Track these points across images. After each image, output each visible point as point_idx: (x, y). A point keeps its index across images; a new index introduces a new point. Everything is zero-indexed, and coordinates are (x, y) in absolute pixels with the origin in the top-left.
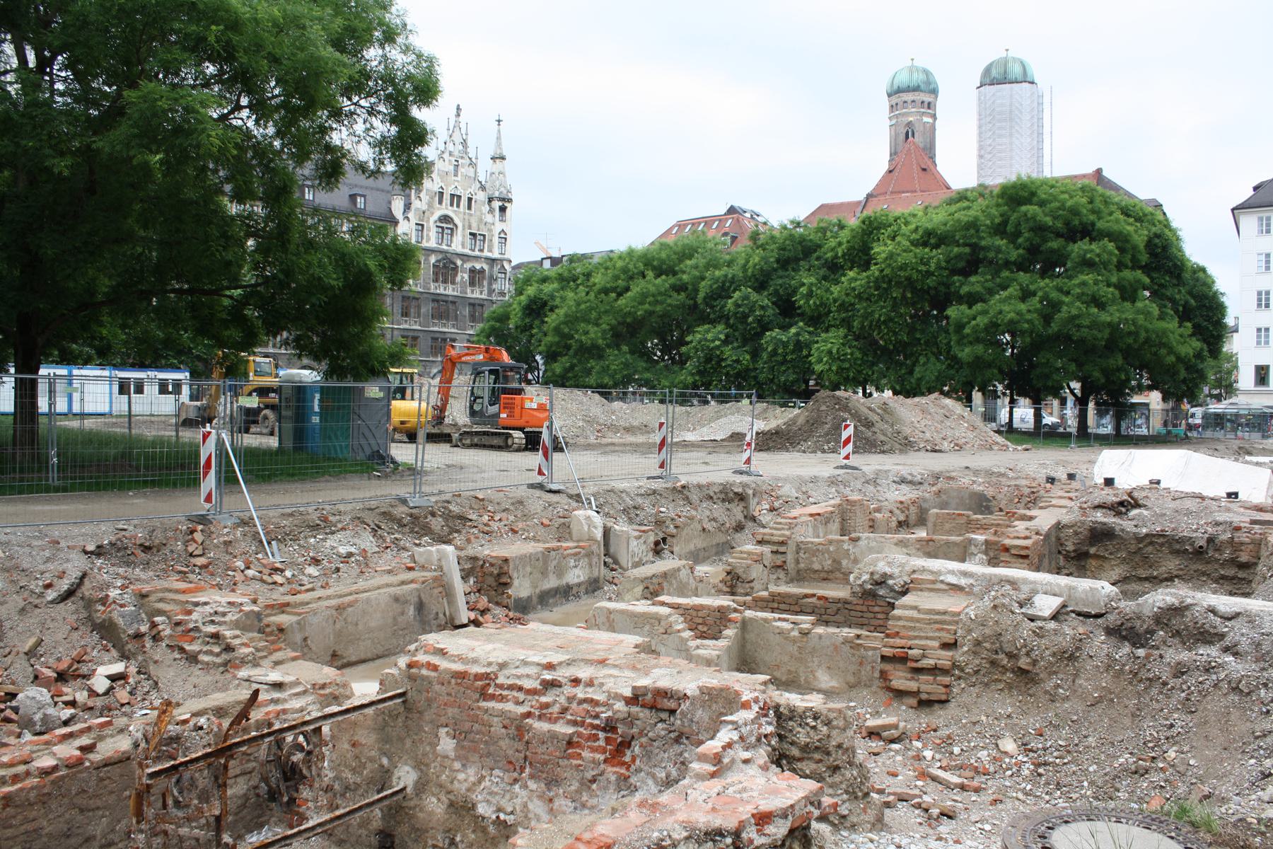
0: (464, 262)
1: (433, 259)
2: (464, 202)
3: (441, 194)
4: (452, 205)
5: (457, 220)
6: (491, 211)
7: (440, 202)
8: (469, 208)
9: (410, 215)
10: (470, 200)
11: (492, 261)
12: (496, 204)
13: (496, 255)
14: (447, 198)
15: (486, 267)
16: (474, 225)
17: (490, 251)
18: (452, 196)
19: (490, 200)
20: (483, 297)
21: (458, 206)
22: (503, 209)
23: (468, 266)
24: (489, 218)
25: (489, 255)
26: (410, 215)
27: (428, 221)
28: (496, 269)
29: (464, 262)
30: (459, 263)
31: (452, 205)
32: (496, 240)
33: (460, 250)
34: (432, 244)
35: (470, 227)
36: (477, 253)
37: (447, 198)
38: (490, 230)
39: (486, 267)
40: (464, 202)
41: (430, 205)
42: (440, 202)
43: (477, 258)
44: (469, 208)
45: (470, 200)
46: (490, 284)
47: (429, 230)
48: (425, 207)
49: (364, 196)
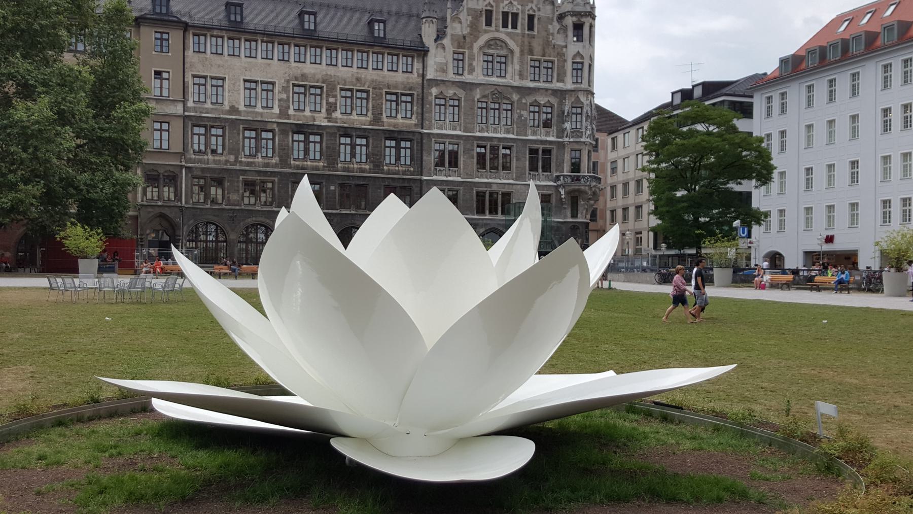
1: (477, 94)
2: (522, 21)
3: (489, 14)
4: (505, 25)
5: (512, 44)
6: (564, 29)
7: (489, 23)
8: (531, 27)
10: (531, 18)
12: (569, 21)
13: (569, 85)
14: (497, 19)
16: (537, 48)
18: (505, 15)
19: (561, 17)
21: (514, 26)
22: (578, 27)
23: (529, 100)
26: (446, 41)
27: (471, 48)
30: (515, 97)
32: (569, 66)
33: (517, 83)
34: (477, 77)
35: (531, 52)
36: (541, 85)
37: (497, 19)
38: (561, 55)
40: (522, 21)
41: (474, 27)
42: (489, 23)
44: (531, 27)
45: (531, 18)
47: (472, 58)
48: (466, 31)
49: (384, 22)
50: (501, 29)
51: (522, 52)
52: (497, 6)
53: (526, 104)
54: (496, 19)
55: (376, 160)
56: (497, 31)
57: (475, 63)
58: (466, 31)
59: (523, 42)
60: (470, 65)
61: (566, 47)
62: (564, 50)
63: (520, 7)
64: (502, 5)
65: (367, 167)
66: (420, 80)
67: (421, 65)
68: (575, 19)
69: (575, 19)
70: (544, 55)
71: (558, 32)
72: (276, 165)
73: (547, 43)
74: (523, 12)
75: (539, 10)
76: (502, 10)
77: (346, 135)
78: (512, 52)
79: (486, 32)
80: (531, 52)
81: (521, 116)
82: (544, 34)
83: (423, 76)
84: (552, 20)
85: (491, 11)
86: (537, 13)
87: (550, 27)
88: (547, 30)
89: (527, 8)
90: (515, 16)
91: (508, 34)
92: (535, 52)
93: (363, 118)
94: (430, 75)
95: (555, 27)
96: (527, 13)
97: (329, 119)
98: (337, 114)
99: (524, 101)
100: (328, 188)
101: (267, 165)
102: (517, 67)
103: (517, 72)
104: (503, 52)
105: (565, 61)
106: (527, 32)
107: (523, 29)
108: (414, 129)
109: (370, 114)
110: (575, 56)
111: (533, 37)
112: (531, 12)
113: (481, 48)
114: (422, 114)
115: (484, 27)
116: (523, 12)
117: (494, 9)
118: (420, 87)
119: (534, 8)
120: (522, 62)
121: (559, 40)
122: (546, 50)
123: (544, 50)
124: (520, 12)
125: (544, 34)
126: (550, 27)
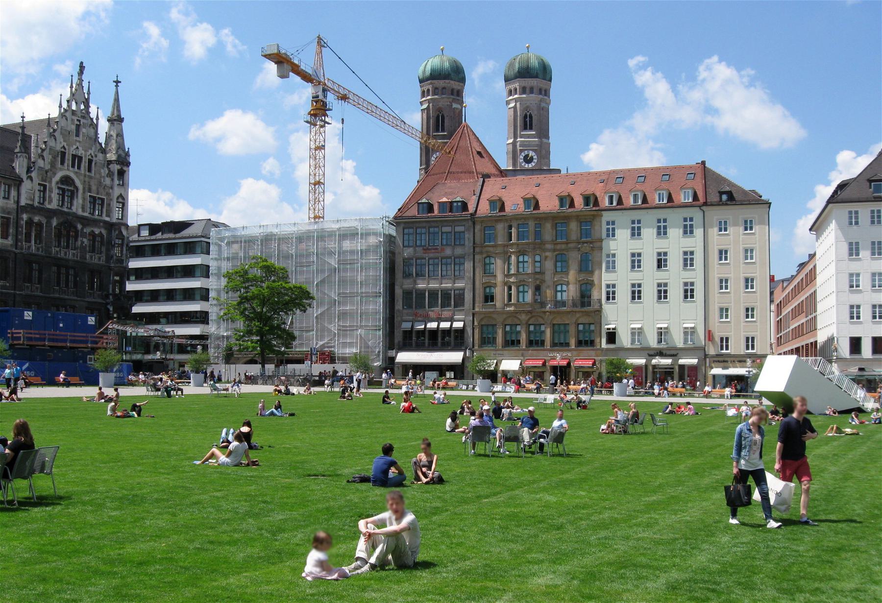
0: (84, 226)
2: (84, 164)
3: (63, 154)
4: (73, 166)
5: (78, 183)
6: (110, 174)
7: (62, 163)
9: (33, 175)
10: (90, 161)
11: (110, 226)
12: (116, 168)
15: (104, 232)
16: (94, 188)
17: (108, 215)
20: (103, 261)
21: (79, 168)
23: (87, 230)
24: (108, 181)
25: (107, 219)
26: (33, 175)
27: (50, 182)
28: (115, 234)
29: (84, 226)
30: (79, 227)
31: (73, 166)
33: (80, 212)
34: (54, 205)
38: (108, 194)
39: (104, 232)
40: (84, 164)
41: (53, 164)
42: (62, 163)
43: (95, 222)
44: (90, 170)
45: (90, 161)
46: (108, 250)
50: (71, 169)
51: (84, 189)
56: (68, 169)
57: (53, 195)
58: (48, 167)
60: (50, 197)
61: (112, 188)
64: (72, 149)
66: (15, 206)
67: (16, 193)
68: (119, 167)
69: (119, 167)
70: (98, 194)
75: (96, 156)
79: (61, 170)
80: (90, 192)
81: (83, 242)
82: (98, 176)
83: (18, 202)
85: (65, 153)
86: (94, 159)
88: (100, 174)
89: (88, 153)
90: (80, 158)
91: (76, 173)
94: (23, 202)
102: (80, 201)
104: (72, 188)
105: (111, 200)
108: (9, 248)
110: (118, 198)
111: (91, 177)
113: (57, 183)
114: (17, 237)
115: (59, 166)
118: (15, 212)
120: (84, 199)
126: (102, 171)
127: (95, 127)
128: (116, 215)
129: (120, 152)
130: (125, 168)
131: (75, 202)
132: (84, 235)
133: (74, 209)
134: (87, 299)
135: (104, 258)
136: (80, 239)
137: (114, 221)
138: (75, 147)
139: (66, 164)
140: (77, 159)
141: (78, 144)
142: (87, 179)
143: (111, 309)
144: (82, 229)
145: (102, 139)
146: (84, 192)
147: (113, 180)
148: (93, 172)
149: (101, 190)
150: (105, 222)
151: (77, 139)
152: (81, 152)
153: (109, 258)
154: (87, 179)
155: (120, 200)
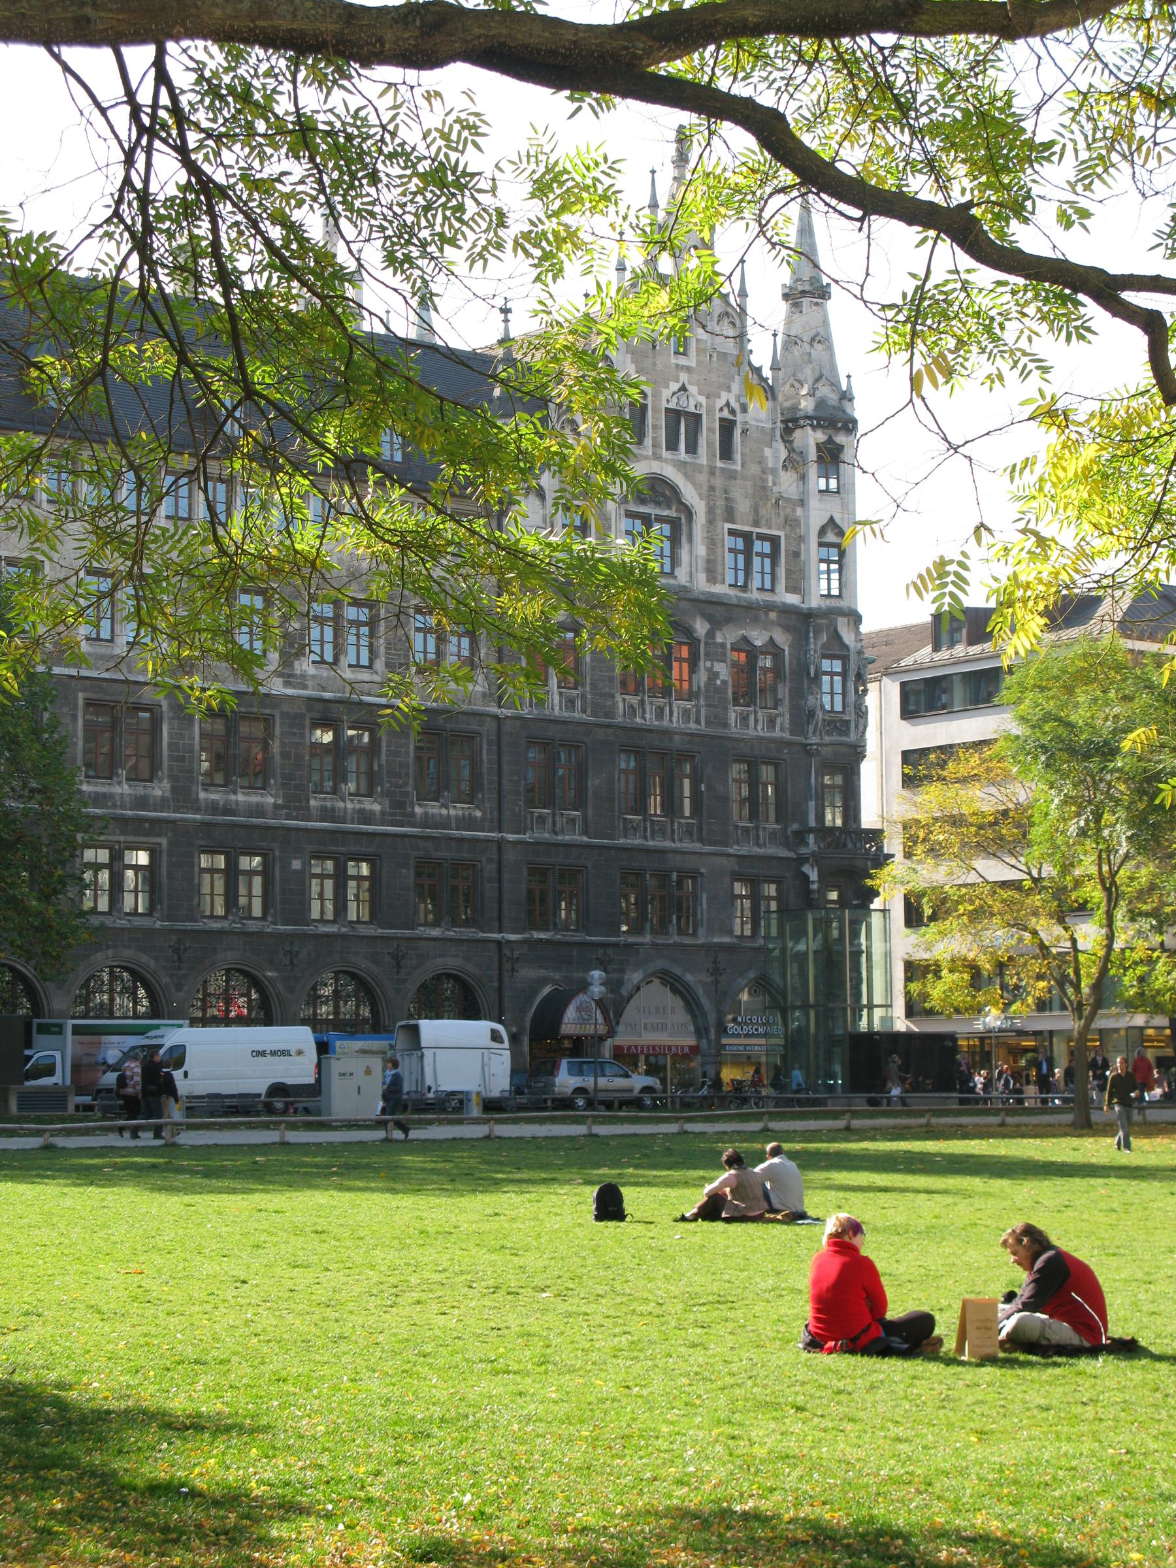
0: (716, 624)
2: (709, 436)
3: (640, 412)
4: (672, 445)
5: (690, 494)
6: (794, 461)
8: (726, 452)
10: (727, 427)
11: (802, 621)
12: (810, 439)
15: (783, 639)
16: (743, 506)
17: (793, 588)
18: (674, 416)
20: (781, 731)
21: (692, 448)
23: (727, 636)
24: (787, 483)
25: (792, 599)
28: (816, 644)
29: (716, 624)
30: (701, 627)
31: (672, 445)
33: (701, 584)
35: (730, 516)
38: (791, 523)
39: (783, 639)
40: (709, 436)
43: (752, 612)
44: (726, 452)
45: (727, 427)
46: (798, 694)
50: (665, 454)
51: (710, 511)
52: (657, 395)
53: (723, 645)
54: (655, 427)
55: (286, 897)
56: (657, 457)
59: (712, 488)
61: (802, 503)
62: (799, 511)
63: (702, 399)
64: (666, 393)
65: (377, 807)
68: (821, 436)
69: (821, 436)
70: (756, 524)
71: (785, 467)
72: (163, 804)
73: (761, 491)
74: (710, 411)
75: (744, 409)
76: (664, 405)
77: (325, 722)
78: (689, 512)
80: (730, 516)
81: (713, 675)
82: (754, 469)
84: (773, 436)
85: (644, 408)
86: (740, 418)
87: (768, 452)
88: (761, 461)
89: (720, 403)
91: (681, 466)
92: (738, 516)
93: (366, 676)
95: (776, 453)
96: (718, 415)
97: (290, 679)
98: (305, 666)
99: (719, 640)
100: (286, 866)
101: (141, 802)
102: (701, 550)
103: (701, 564)
104: (672, 513)
105: (801, 539)
106: (719, 464)
107: (711, 455)
108: (479, 707)
109: (379, 664)
110: (822, 531)
111: (731, 475)
112: (726, 414)
116: (710, 411)
117: (649, 402)
119: (733, 403)
121: (787, 483)
122: (762, 512)
123: (756, 511)
124: (703, 411)
125: (754, 469)
126: (768, 452)
127: (736, 317)
128: (822, 584)
129: (824, 391)
130: (840, 439)
131: (684, 554)
132: (717, 654)
133: (682, 576)
134: (733, 850)
135: (784, 719)
136: (704, 664)
137: (814, 602)
138: (675, 386)
139: (648, 441)
140: (682, 425)
141: (684, 377)
142: (718, 482)
143: (814, 875)
144: (710, 634)
145: (762, 353)
146: (711, 522)
147: (803, 477)
148: (738, 457)
149: (766, 511)
150: (787, 611)
151: (682, 361)
152: (695, 401)
153: (803, 717)
154: (718, 482)
155: (831, 537)
